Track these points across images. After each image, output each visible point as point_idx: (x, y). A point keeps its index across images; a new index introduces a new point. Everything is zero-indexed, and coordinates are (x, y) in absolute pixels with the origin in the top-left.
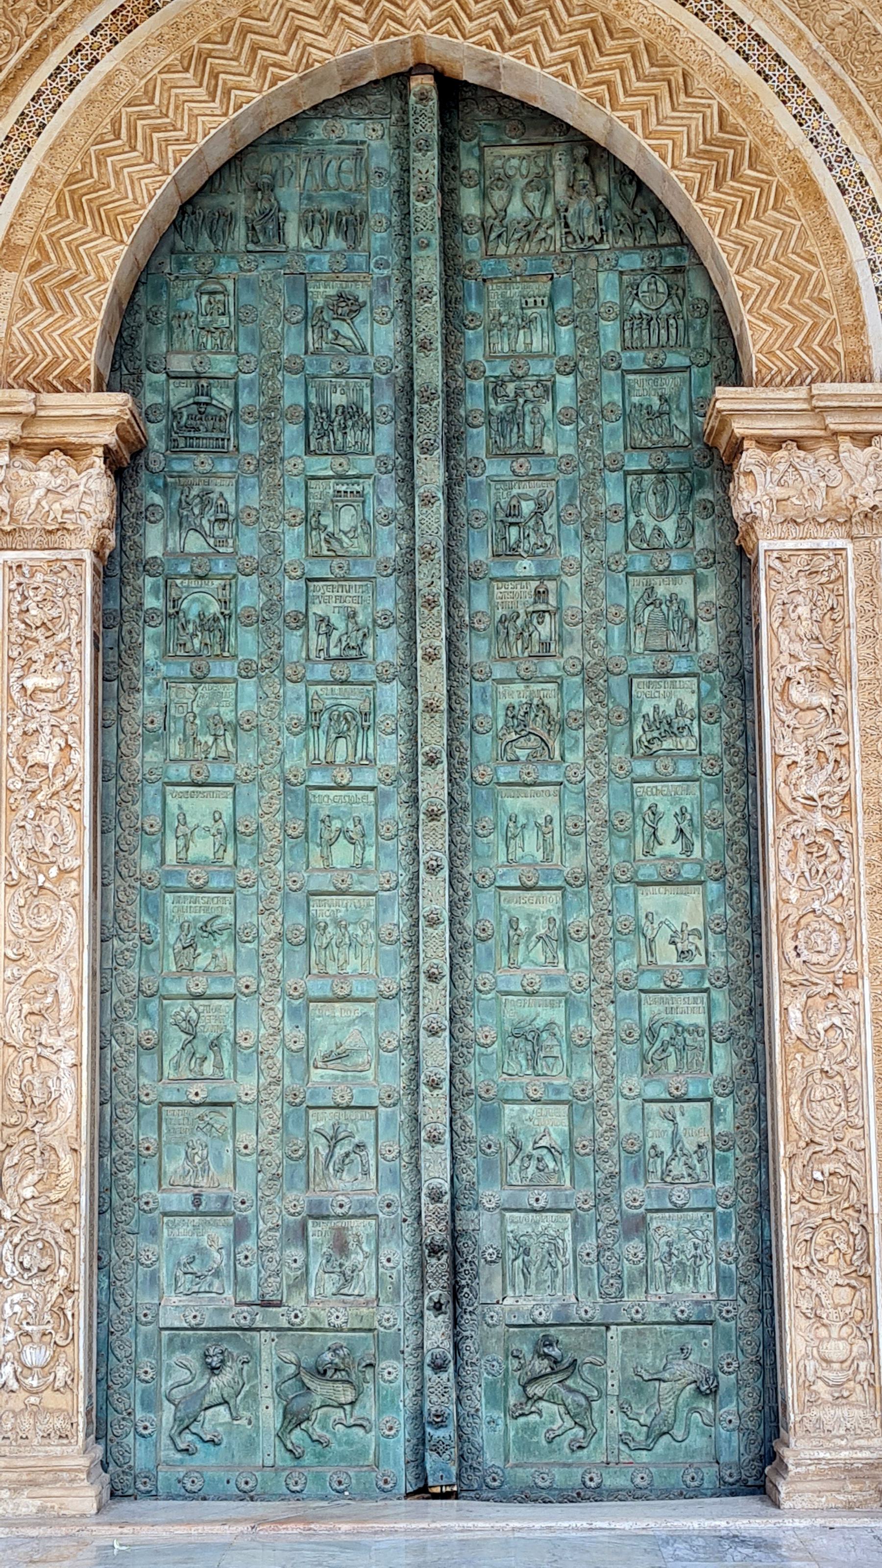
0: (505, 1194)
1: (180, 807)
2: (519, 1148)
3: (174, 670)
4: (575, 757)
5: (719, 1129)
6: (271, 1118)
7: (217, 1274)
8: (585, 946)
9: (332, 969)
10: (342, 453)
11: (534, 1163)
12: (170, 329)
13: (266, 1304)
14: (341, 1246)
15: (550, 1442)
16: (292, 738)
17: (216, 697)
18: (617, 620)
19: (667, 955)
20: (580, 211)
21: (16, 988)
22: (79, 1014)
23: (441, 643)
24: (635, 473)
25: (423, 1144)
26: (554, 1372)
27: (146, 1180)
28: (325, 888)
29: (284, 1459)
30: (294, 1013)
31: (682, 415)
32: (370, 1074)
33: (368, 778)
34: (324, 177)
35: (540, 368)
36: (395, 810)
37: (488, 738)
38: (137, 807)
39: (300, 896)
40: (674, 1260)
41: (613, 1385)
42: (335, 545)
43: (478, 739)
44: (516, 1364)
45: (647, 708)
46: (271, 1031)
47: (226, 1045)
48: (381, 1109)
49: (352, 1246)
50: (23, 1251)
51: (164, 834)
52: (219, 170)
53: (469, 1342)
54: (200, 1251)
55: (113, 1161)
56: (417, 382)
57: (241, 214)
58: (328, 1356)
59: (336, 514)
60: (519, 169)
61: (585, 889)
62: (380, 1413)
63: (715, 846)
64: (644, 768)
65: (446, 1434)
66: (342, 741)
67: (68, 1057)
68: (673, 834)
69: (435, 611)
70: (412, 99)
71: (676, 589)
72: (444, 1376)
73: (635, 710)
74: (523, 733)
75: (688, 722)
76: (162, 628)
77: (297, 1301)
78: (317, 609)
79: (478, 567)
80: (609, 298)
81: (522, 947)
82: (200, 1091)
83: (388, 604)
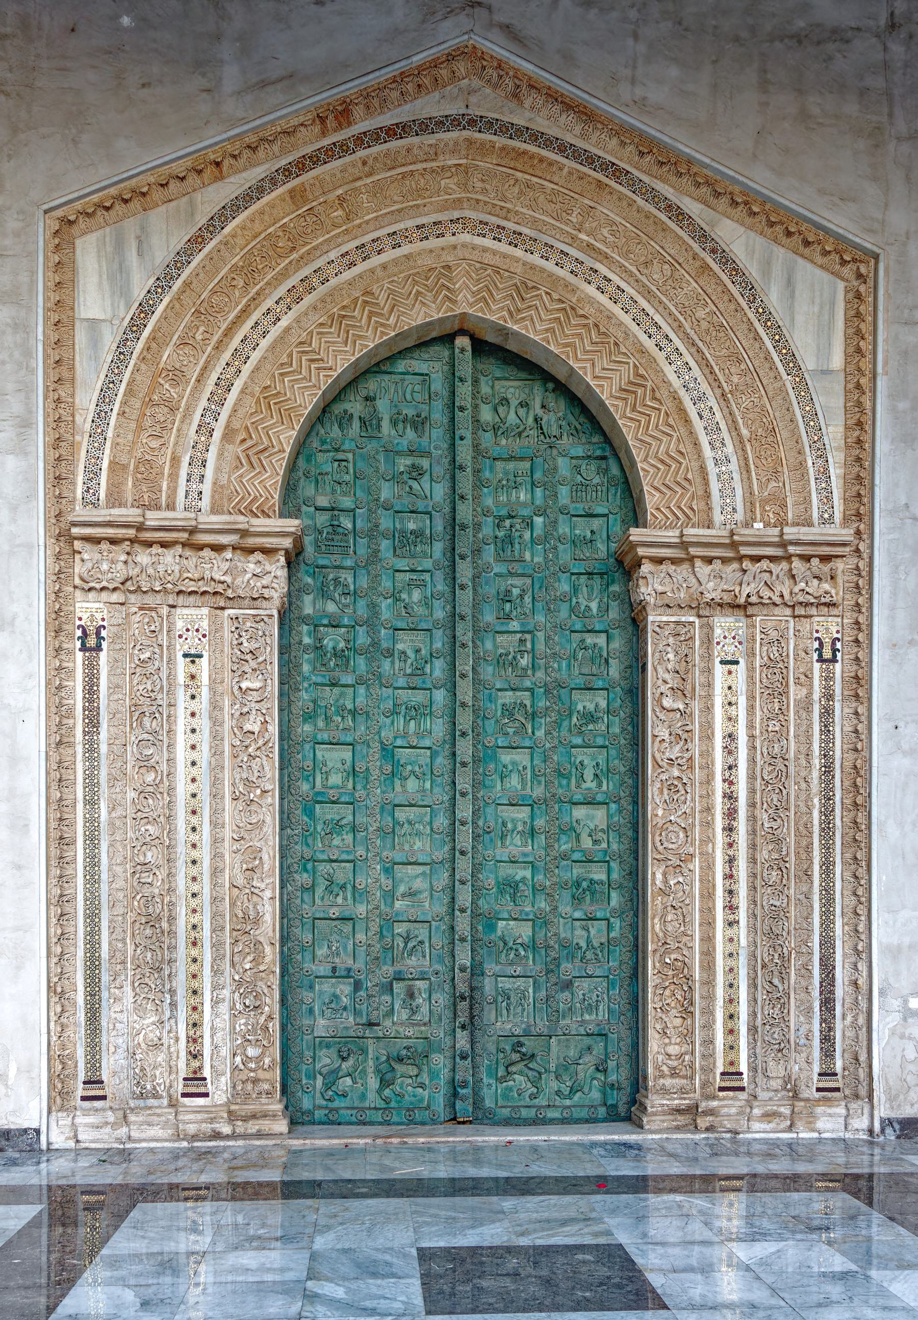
0: (498, 968)
2: (505, 944)
3: (319, 680)
4: (540, 733)
5: (612, 935)
6: (374, 927)
7: (345, 1009)
9: (407, 847)
10: (413, 557)
11: (513, 952)
12: (317, 481)
13: (371, 1024)
14: (411, 995)
17: (342, 695)
19: (587, 843)
20: (549, 421)
21: (239, 856)
22: (274, 871)
23: (469, 668)
26: (522, 1060)
27: (307, 959)
30: (386, 870)
31: (603, 542)
32: (427, 904)
33: (427, 743)
35: (525, 512)
36: (441, 761)
38: (300, 756)
39: (390, 807)
42: (410, 610)
43: (486, 722)
44: (502, 1055)
47: (349, 887)
50: (245, 998)
52: (344, 388)
54: (336, 997)
55: (289, 949)
56: (458, 517)
58: (404, 1052)
62: (431, 1080)
63: (614, 785)
64: (578, 741)
66: (412, 722)
67: (268, 894)
68: (592, 777)
70: (457, 351)
77: (388, 1023)
79: (488, 624)
82: (334, 912)
83: (438, 645)
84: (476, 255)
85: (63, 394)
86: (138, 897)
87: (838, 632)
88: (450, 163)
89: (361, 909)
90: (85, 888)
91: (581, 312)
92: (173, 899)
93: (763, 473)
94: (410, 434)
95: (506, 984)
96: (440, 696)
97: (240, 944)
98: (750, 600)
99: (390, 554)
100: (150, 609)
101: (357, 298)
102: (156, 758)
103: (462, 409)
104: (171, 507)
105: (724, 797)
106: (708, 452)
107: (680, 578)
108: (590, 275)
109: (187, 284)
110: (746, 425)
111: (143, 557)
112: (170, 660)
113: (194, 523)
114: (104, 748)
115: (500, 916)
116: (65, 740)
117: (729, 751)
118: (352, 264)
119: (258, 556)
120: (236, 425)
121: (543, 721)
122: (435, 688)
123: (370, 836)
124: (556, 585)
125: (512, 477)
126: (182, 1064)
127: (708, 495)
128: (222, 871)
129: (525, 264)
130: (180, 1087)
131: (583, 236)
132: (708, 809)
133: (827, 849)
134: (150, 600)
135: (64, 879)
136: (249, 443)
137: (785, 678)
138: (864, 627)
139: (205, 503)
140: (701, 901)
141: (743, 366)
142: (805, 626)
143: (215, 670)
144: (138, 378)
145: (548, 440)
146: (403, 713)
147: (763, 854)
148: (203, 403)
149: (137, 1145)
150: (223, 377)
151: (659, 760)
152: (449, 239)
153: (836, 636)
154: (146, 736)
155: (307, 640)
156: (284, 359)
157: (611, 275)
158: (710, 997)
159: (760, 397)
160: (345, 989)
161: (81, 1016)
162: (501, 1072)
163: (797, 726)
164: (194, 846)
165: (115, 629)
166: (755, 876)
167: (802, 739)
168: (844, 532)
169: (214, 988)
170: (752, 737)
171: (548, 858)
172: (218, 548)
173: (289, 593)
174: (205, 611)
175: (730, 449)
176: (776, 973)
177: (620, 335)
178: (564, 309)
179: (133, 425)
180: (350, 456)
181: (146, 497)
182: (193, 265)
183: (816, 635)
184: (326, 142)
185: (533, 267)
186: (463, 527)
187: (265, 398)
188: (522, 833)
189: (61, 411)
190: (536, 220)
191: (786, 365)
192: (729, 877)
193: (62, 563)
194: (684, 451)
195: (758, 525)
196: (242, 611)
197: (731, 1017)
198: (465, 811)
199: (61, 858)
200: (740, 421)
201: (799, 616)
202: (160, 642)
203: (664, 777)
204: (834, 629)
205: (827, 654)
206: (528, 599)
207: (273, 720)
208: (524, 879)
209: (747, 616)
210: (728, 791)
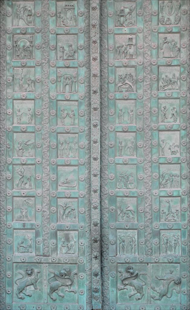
1: (18, 107)
6: (46, 201)
7: (30, 247)
8: (142, 149)
11: (126, 215)
14: (67, 239)
15: (130, 297)
16: (52, 85)
18: (155, 47)
23: (98, 55)
25: (92, 209)
28: (63, 132)
29: (51, 301)
33: (76, 98)
36: (83, 108)
37: (113, 85)
38: (5, 107)
39: (55, 133)
40: (168, 244)
41: (149, 280)
44: (119, 274)
45: (163, 76)
46: (46, 175)
47: (33, 179)
49: (71, 239)
51: (13, 115)
53: (106, 268)
54: (24, 240)
58: (63, 271)
59: (66, 14)
61: (143, 132)
62: (79, 288)
65: (98, 294)
66: (67, 86)
68: (170, 116)
69: (96, 45)
73: (160, 76)
74: (124, 83)
75: (176, 80)
76: (12, 51)
77: (54, 255)
78: (60, 44)
81: (123, 150)
89: (39, 191)
96: (83, 72)
115: (118, 195)
121: (142, 84)
122: (80, 66)
160: (30, 235)
208: (131, 175)
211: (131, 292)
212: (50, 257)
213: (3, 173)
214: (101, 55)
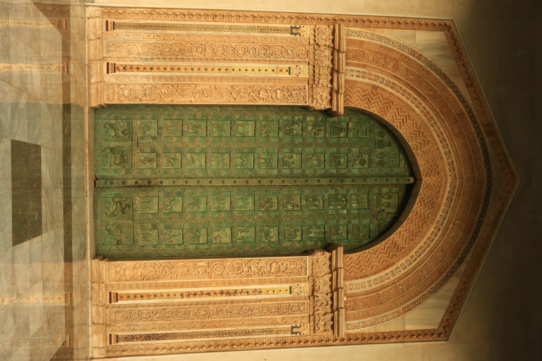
3: (281, 123)
4: (260, 214)
6: (179, 145)
7: (144, 133)
9: (213, 159)
10: (330, 161)
14: (150, 160)
15: (107, 207)
22: (202, 102)
23: (286, 184)
24: (325, 227)
31: (337, 238)
32: (189, 167)
33: (256, 167)
34: (392, 158)
35: (348, 206)
37: (265, 194)
38: (250, 114)
39: (229, 152)
41: (120, 221)
42: (309, 160)
43: (265, 192)
44: (124, 199)
45: (271, 230)
47: (196, 134)
48: (181, 170)
49: (150, 163)
54: (149, 129)
55: (170, 109)
56: (346, 179)
57: (383, 139)
58: (126, 158)
60: (393, 201)
61: (230, 216)
62: (113, 169)
67: (193, 100)
70: (408, 178)
71: (298, 237)
72: (121, 184)
77: (138, 151)
80: (364, 221)
82: (185, 128)
83: (295, 171)
84: (443, 184)
85: (388, 24)
86: (192, 46)
87: (304, 334)
88: (476, 174)
89: (186, 140)
90: (195, 25)
91: (424, 226)
92: (191, 61)
93: (365, 300)
94: (377, 160)
95: (155, 200)
96: (275, 172)
97: (172, 88)
98: (316, 297)
99: (330, 152)
100: (307, 55)
101: (426, 138)
102: (249, 55)
103: (387, 180)
104: (347, 64)
105: (235, 290)
106: (373, 278)
107: (324, 268)
108: (437, 229)
109: (429, 72)
110: (384, 292)
111: (328, 52)
112: (287, 61)
113: (341, 72)
114: (252, 34)
116: (255, 19)
117: (255, 291)
118: (439, 137)
119: (329, 98)
120: (379, 90)
121: (266, 215)
123: (217, 143)
124: (320, 219)
125: (361, 201)
126: (121, 63)
127: (356, 278)
128: (202, 81)
129: (441, 203)
130: (111, 62)
131: (451, 225)
132: (230, 284)
133: (215, 334)
134: (311, 55)
135: (199, 16)
136: (372, 95)
137: (284, 313)
138: (306, 344)
139: (349, 78)
140: (191, 282)
141: (405, 290)
142: (306, 320)
143: (285, 79)
144: (395, 53)
145: (376, 215)
146: (268, 157)
147: (211, 307)
148: (386, 78)
149: (87, 43)
150: (396, 86)
151: (250, 262)
152: (449, 173)
153: (302, 333)
154: (257, 51)
155: (296, 118)
156: (403, 110)
157: (437, 237)
158: (150, 287)
159: (394, 298)
160: (153, 132)
161: (142, 22)
162: (117, 200)
163: (265, 319)
164: (213, 69)
165: (299, 40)
166: (203, 304)
167: (260, 322)
168: (343, 334)
169: (153, 77)
170: (260, 301)
171: (209, 218)
172: (332, 82)
173: (315, 110)
174: (307, 76)
175: (374, 286)
176: (161, 315)
177: (416, 241)
178: (425, 219)
179: (377, 50)
180: (368, 136)
181: (350, 54)
182: (436, 75)
183: (302, 325)
184: (481, 127)
185: (439, 206)
186: (342, 181)
187: (389, 102)
188: (219, 207)
189: (382, 23)
190: (456, 207)
191: (406, 307)
192: (202, 293)
193: (324, 21)
194: (373, 268)
195: (345, 299)
196: (307, 91)
197: (142, 296)
198: (228, 182)
199: (208, 16)
200: (385, 290)
201: (310, 318)
202: (295, 58)
203: (243, 264)
204: (305, 332)
205: (295, 330)
206: (314, 208)
207: (264, 103)
208: (199, 208)
209: (309, 297)
210: (238, 292)
211: (112, 208)
212: (136, 147)
213: (200, 113)
214: (286, 186)
